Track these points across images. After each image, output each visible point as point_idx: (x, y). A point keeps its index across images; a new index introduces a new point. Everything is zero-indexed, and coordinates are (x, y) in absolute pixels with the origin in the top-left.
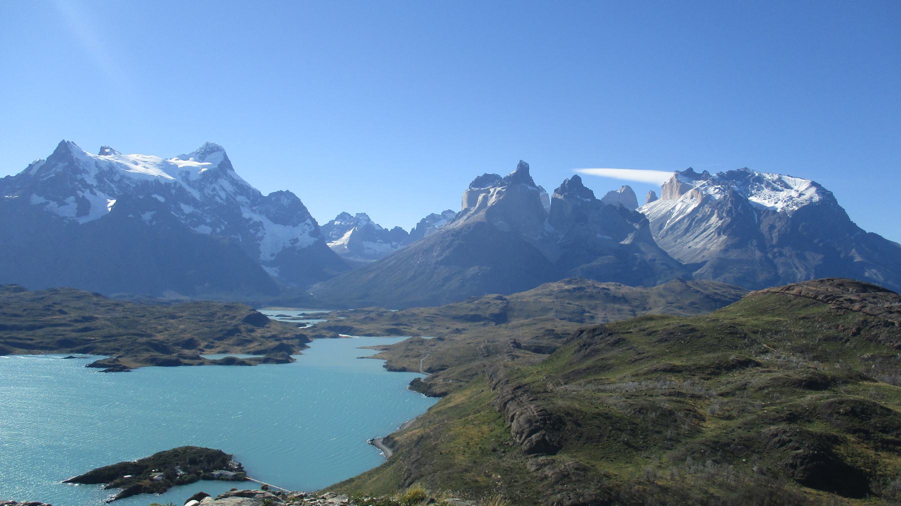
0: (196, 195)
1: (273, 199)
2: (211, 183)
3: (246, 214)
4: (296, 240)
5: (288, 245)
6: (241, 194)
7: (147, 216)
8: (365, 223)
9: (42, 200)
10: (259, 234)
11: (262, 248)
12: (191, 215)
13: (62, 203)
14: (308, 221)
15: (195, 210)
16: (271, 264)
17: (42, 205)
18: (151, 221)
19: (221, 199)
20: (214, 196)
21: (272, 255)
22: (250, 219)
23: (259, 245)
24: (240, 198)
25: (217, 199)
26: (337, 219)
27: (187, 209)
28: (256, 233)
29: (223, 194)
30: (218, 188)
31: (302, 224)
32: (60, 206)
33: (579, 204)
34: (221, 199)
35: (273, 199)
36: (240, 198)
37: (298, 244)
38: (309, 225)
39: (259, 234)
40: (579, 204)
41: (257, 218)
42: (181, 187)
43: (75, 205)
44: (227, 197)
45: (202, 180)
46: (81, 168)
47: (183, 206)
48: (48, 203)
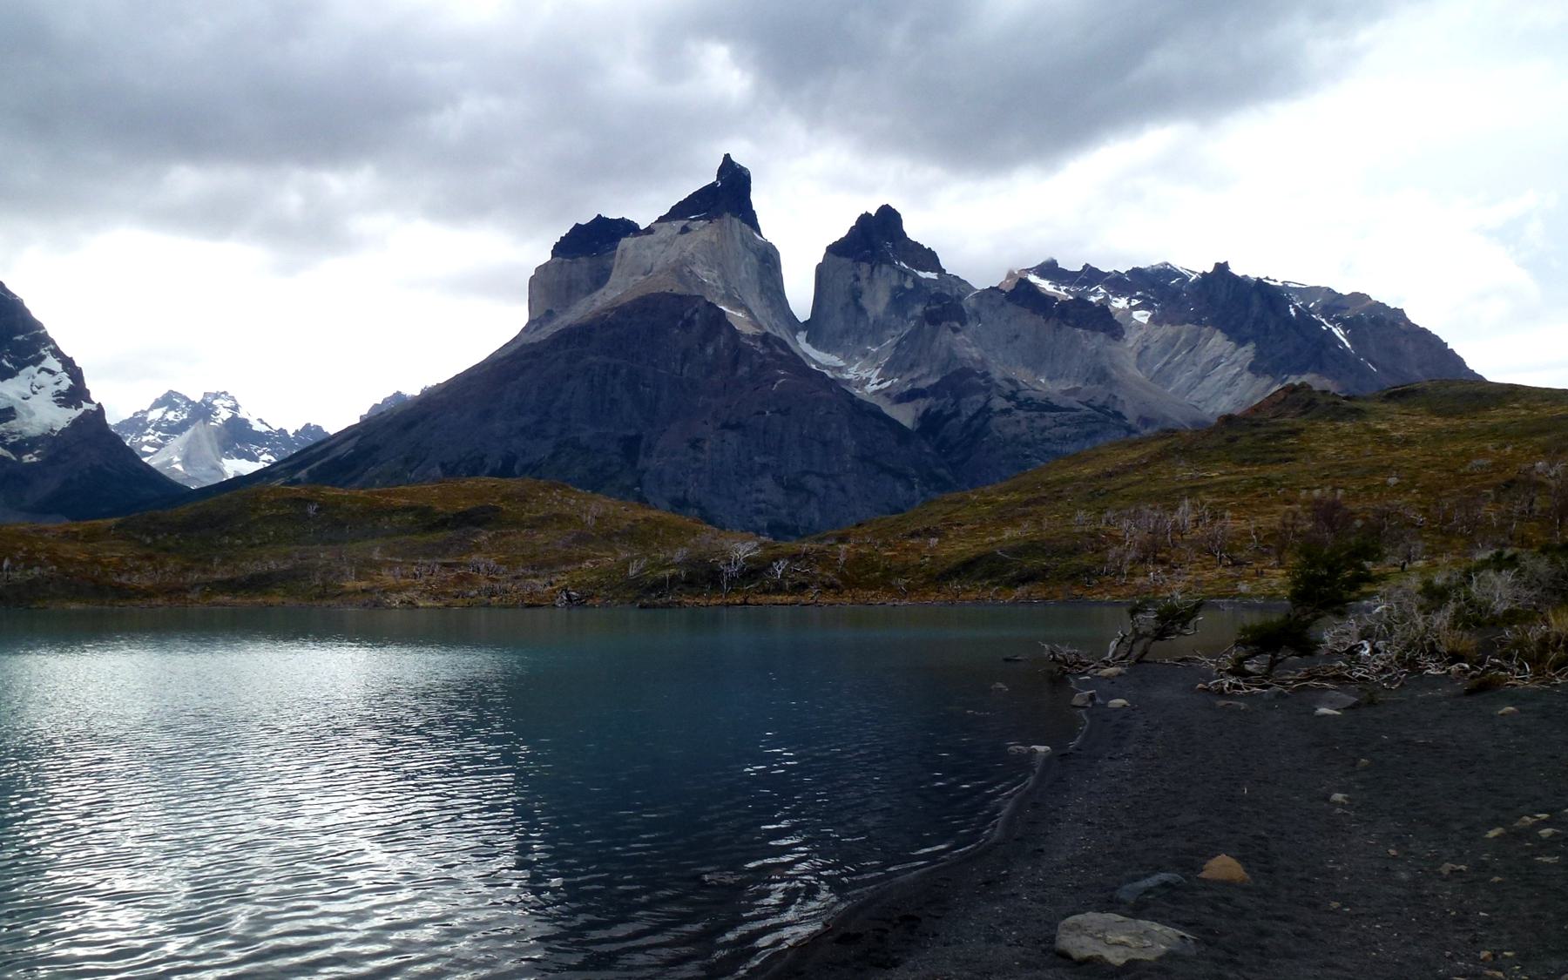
8: (225, 415)
14: (52, 363)
26: (157, 404)
31: (32, 369)
33: (909, 285)
38: (51, 372)
40: (909, 285)
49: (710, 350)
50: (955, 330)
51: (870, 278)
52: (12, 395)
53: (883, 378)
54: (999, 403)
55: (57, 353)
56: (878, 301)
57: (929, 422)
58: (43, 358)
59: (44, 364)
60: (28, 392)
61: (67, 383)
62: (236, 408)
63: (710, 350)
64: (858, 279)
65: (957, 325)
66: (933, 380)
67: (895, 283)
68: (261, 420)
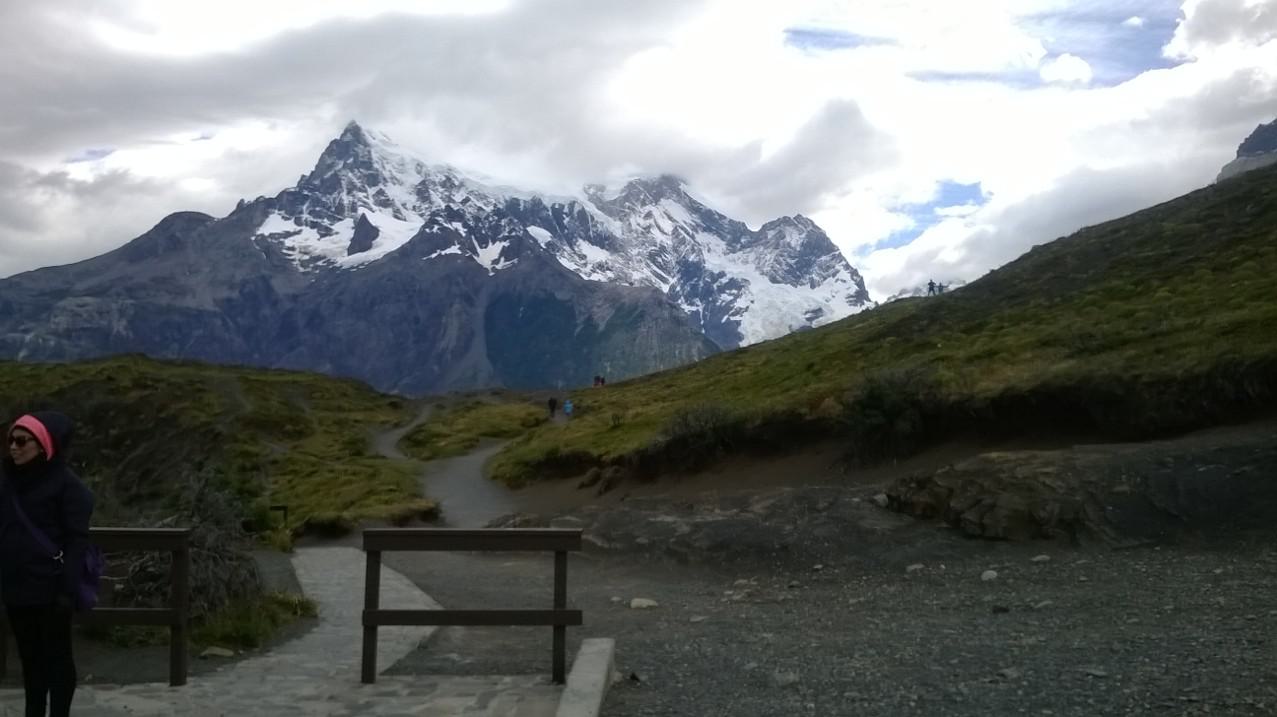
1: (771, 234)
2: (644, 204)
4: (818, 312)
6: (704, 230)
7: (488, 255)
9: (290, 226)
10: (740, 303)
12: (601, 267)
13: (326, 232)
14: (845, 275)
17: (288, 234)
18: (496, 262)
20: (648, 229)
22: (722, 274)
23: (738, 323)
27: (596, 254)
29: (668, 226)
30: (656, 211)
31: (831, 280)
32: (322, 236)
35: (771, 234)
38: (845, 281)
39: (740, 303)
42: (583, 213)
43: (351, 233)
44: (675, 229)
45: (626, 198)
46: (386, 174)
47: (584, 247)
48: (298, 233)
52: (820, 300)
55: (847, 267)
58: (838, 272)
59: (838, 276)
60: (830, 297)
61: (854, 288)
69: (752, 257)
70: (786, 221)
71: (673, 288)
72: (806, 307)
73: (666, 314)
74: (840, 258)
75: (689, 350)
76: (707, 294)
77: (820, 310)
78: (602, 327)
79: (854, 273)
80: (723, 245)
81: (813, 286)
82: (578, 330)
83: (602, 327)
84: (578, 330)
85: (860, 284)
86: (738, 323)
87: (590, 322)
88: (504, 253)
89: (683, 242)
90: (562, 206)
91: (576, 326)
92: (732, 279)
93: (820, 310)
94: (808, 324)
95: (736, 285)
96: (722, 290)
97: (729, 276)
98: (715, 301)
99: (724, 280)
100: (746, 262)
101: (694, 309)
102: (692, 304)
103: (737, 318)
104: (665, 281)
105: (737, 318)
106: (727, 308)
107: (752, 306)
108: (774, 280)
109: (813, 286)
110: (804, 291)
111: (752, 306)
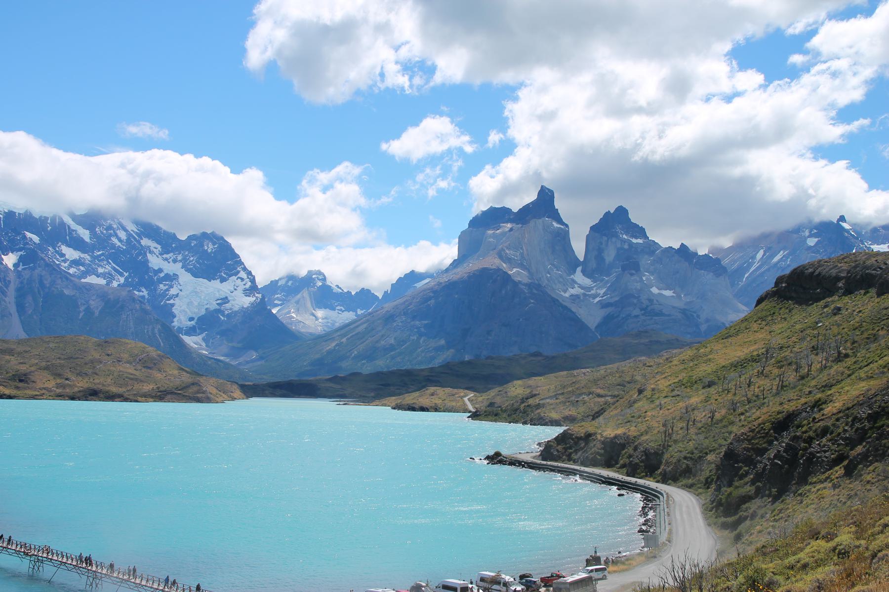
0: (85, 234)
3: (155, 261)
4: (225, 300)
5: (213, 306)
6: (149, 237)
10: (173, 291)
11: (174, 310)
12: (76, 263)
14: (243, 274)
15: (82, 255)
16: (191, 331)
19: (120, 240)
21: (191, 319)
22: (160, 270)
23: (173, 305)
24: (145, 242)
25: (115, 240)
27: (71, 254)
28: (167, 290)
31: (234, 278)
33: (626, 247)
34: (120, 240)
36: (145, 242)
37: (228, 306)
38: (242, 279)
40: (626, 247)
41: (170, 268)
44: (128, 239)
47: (65, 249)
49: (503, 292)
50: (632, 275)
51: (607, 245)
53: (605, 294)
54: (637, 312)
55: (245, 269)
56: (610, 255)
57: (607, 319)
58: (239, 272)
59: (239, 275)
62: (324, 279)
63: (503, 292)
64: (601, 243)
65: (634, 272)
66: (617, 299)
67: (619, 245)
68: (337, 286)
69: (180, 258)
70: (205, 235)
71: (126, 279)
72: (218, 296)
73: (138, 306)
74: (241, 263)
75: (153, 329)
76: (150, 284)
77: (226, 298)
78: (97, 313)
79: (249, 273)
80: (159, 247)
81: (222, 282)
82: (81, 315)
83: (97, 313)
84: (81, 315)
85: (253, 280)
86: (173, 305)
87: (88, 311)
88: (21, 260)
89: (134, 247)
90: (46, 218)
91: (79, 312)
92: (167, 275)
93: (226, 298)
94: (218, 307)
95: (172, 278)
96: (161, 281)
97: (166, 272)
98: (155, 290)
99: (162, 275)
100: (175, 261)
101: (141, 294)
102: (139, 291)
103: (172, 301)
104: (121, 275)
105: (172, 301)
106: (164, 294)
107: (181, 293)
108: (195, 275)
109: (222, 282)
110: (216, 283)
111: (181, 293)
